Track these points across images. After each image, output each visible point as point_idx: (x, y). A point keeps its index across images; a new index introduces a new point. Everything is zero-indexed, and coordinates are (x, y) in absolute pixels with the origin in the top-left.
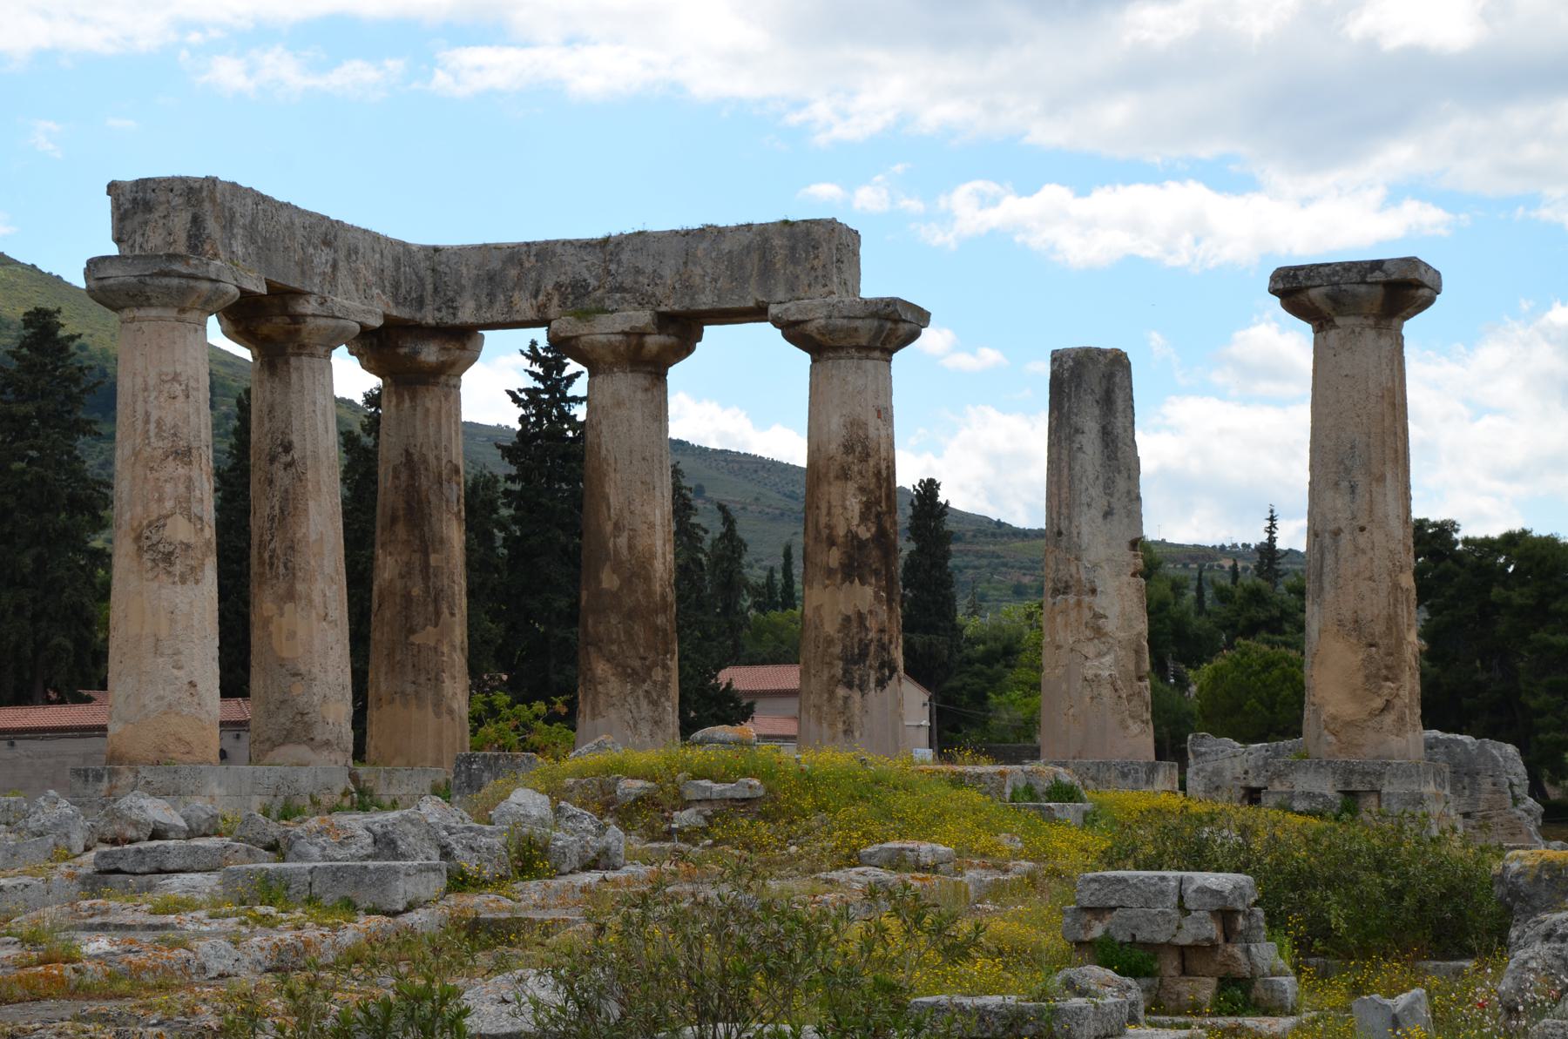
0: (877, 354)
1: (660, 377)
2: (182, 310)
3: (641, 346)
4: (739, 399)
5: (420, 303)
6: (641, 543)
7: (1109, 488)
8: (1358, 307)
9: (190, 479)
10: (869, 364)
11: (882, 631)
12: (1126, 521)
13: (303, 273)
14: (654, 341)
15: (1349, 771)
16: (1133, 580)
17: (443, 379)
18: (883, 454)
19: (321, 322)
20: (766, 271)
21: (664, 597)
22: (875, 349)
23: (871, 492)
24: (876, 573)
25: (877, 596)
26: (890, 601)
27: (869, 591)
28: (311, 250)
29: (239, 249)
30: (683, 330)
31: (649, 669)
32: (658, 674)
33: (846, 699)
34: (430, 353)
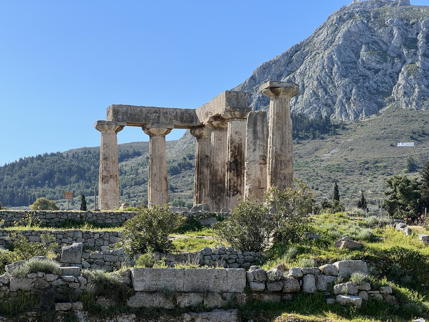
0: (236, 119)
2: (106, 131)
3: (212, 125)
5: (192, 121)
6: (215, 168)
7: (255, 144)
9: (107, 163)
10: (233, 122)
11: (235, 183)
12: (258, 151)
13: (146, 120)
16: (259, 166)
17: (203, 137)
18: (236, 142)
19: (153, 129)
21: (221, 180)
22: (234, 118)
23: (233, 151)
24: (234, 170)
25: (233, 175)
26: (237, 176)
27: (232, 174)
28: (149, 115)
29: (120, 117)
31: (216, 197)
32: (218, 197)
33: (227, 199)
34: (197, 132)
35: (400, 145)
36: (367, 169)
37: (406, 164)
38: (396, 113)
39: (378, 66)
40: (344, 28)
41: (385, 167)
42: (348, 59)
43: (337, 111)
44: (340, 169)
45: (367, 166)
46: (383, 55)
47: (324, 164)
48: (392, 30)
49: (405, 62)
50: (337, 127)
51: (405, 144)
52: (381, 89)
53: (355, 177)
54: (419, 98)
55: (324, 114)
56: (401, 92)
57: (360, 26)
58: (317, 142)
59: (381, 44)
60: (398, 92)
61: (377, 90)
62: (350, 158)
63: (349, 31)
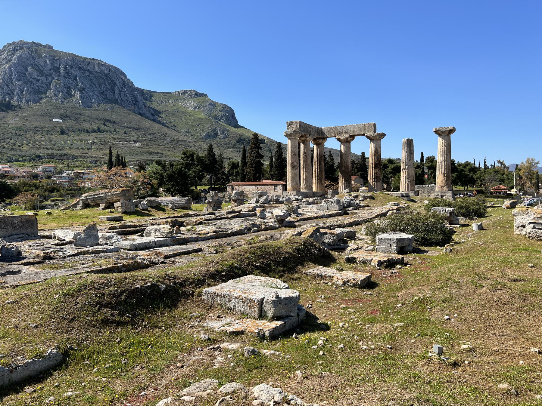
1: (350, 143)
4: (361, 147)
8: (446, 134)
14: (349, 139)
15: (442, 192)
20: (365, 129)
30: (353, 137)
34: (321, 141)
35: (54, 120)
36: (38, 131)
37: (59, 130)
38: (50, 104)
39: (38, 78)
40: (17, 54)
41: (48, 131)
42: (21, 71)
43: (15, 98)
44: (20, 129)
45: (37, 129)
46: (42, 73)
47: (11, 126)
48: (46, 61)
49: (53, 78)
50: (16, 107)
51: (57, 120)
52: (41, 90)
53: (31, 134)
54: (62, 98)
55: (7, 99)
56: (53, 94)
57: (27, 54)
58: (4, 114)
59: (40, 67)
60: (50, 93)
61: (39, 90)
62: (26, 124)
63: (20, 56)
